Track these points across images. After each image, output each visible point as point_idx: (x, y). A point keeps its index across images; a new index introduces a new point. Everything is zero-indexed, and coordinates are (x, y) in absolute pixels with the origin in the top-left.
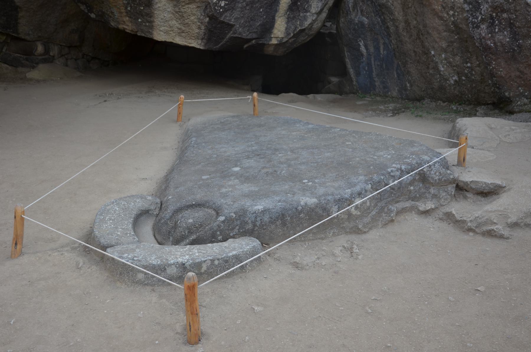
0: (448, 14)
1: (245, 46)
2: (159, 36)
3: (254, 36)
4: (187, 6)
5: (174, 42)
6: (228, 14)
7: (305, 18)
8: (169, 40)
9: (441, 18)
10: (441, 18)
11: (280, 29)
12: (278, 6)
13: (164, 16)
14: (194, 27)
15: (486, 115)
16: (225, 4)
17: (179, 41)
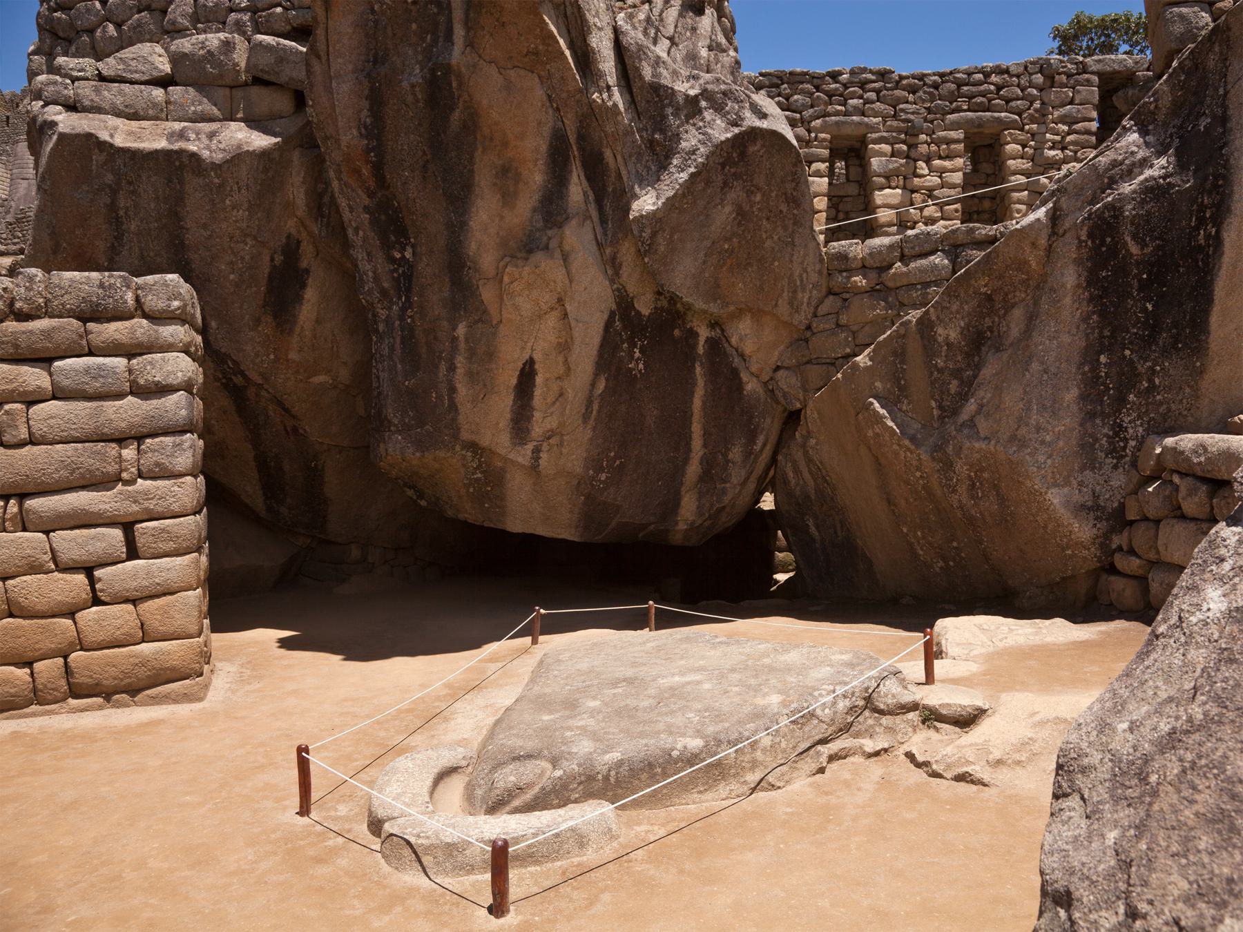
2: (515, 525)
7: (724, 492)
11: (689, 509)
17: (541, 531)
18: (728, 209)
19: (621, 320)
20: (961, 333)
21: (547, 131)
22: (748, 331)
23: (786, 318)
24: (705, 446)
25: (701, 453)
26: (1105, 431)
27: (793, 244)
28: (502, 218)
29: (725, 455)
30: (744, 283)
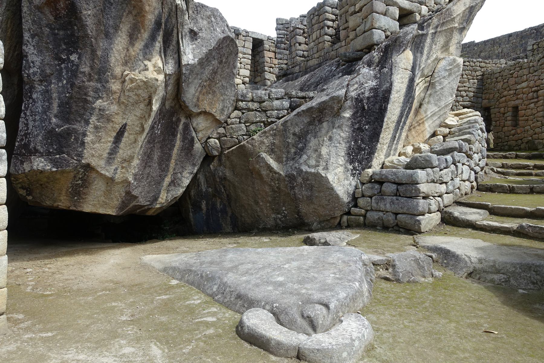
0: (274, 183)
2: (87, 208)
3: (148, 203)
8: (94, 210)
9: (270, 185)
16: (137, 184)
17: (101, 211)
20: (301, 130)
21: (157, 12)
22: (201, 121)
23: (218, 118)
28: (128, 50)
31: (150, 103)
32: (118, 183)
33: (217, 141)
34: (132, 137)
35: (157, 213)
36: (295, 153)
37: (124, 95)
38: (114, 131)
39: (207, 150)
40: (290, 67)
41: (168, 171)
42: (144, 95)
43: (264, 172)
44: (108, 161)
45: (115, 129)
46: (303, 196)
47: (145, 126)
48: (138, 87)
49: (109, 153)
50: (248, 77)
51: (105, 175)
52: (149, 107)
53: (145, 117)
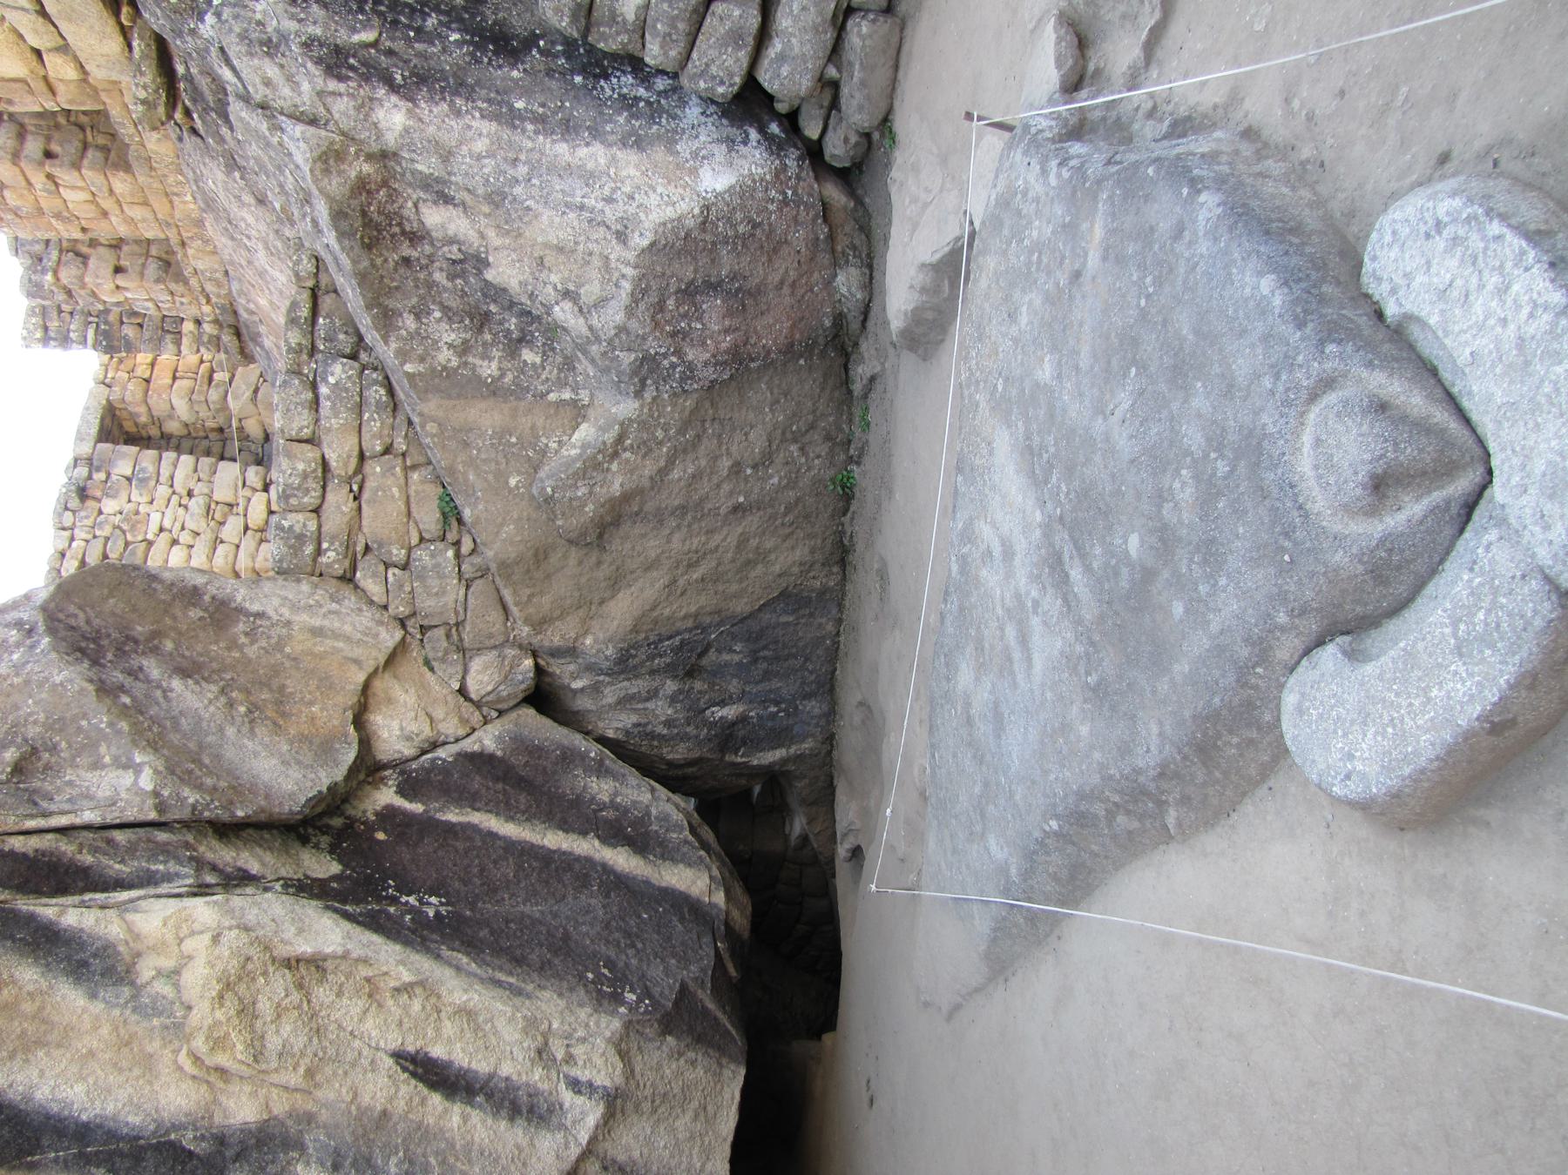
1: (732, 972)
3: (707, 939)
4: (638, 1077)
5: (730, 1138)
6: (656, 991)
7: (664, 818)
10: (670, 463)
12: (634, 878)
13: (665, 1147)
14: (690, 1075)
15: (890, 223)
16: (632, 991)
17: (728, 1122)
18: (176, 684)
19: (344, 902)
22: (395, 724)
24: (584, 833)
25: (597, 843)
26: (621, 120)
27: (260, 615)
29: (603, 807)
30: (311, 703)
31: (317, 963)
32: (629, 1073)
33: (476, 664)
34: (449, 1028)
35: (745, 900)
36: (548, 350)
37: (276, 1070)
38: (423, 1102)
39: (512, 703)
40: (207, 309)
41: (589, 860)
42: (275, 988)
43: (616, 485)
44: (541, 1117)
45: (417, 1100)
46: (727, 331)
47: (407, 977)
48: (247, 1011)
49: (512, 1119)
50: (243, 472)
51: (597, 1127)
52: (329, 965)
53: (368, 980)
